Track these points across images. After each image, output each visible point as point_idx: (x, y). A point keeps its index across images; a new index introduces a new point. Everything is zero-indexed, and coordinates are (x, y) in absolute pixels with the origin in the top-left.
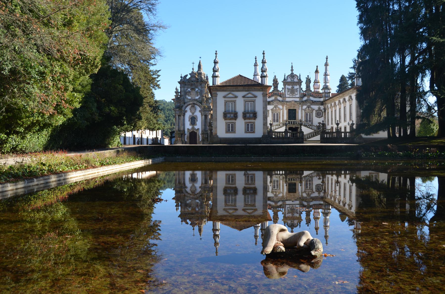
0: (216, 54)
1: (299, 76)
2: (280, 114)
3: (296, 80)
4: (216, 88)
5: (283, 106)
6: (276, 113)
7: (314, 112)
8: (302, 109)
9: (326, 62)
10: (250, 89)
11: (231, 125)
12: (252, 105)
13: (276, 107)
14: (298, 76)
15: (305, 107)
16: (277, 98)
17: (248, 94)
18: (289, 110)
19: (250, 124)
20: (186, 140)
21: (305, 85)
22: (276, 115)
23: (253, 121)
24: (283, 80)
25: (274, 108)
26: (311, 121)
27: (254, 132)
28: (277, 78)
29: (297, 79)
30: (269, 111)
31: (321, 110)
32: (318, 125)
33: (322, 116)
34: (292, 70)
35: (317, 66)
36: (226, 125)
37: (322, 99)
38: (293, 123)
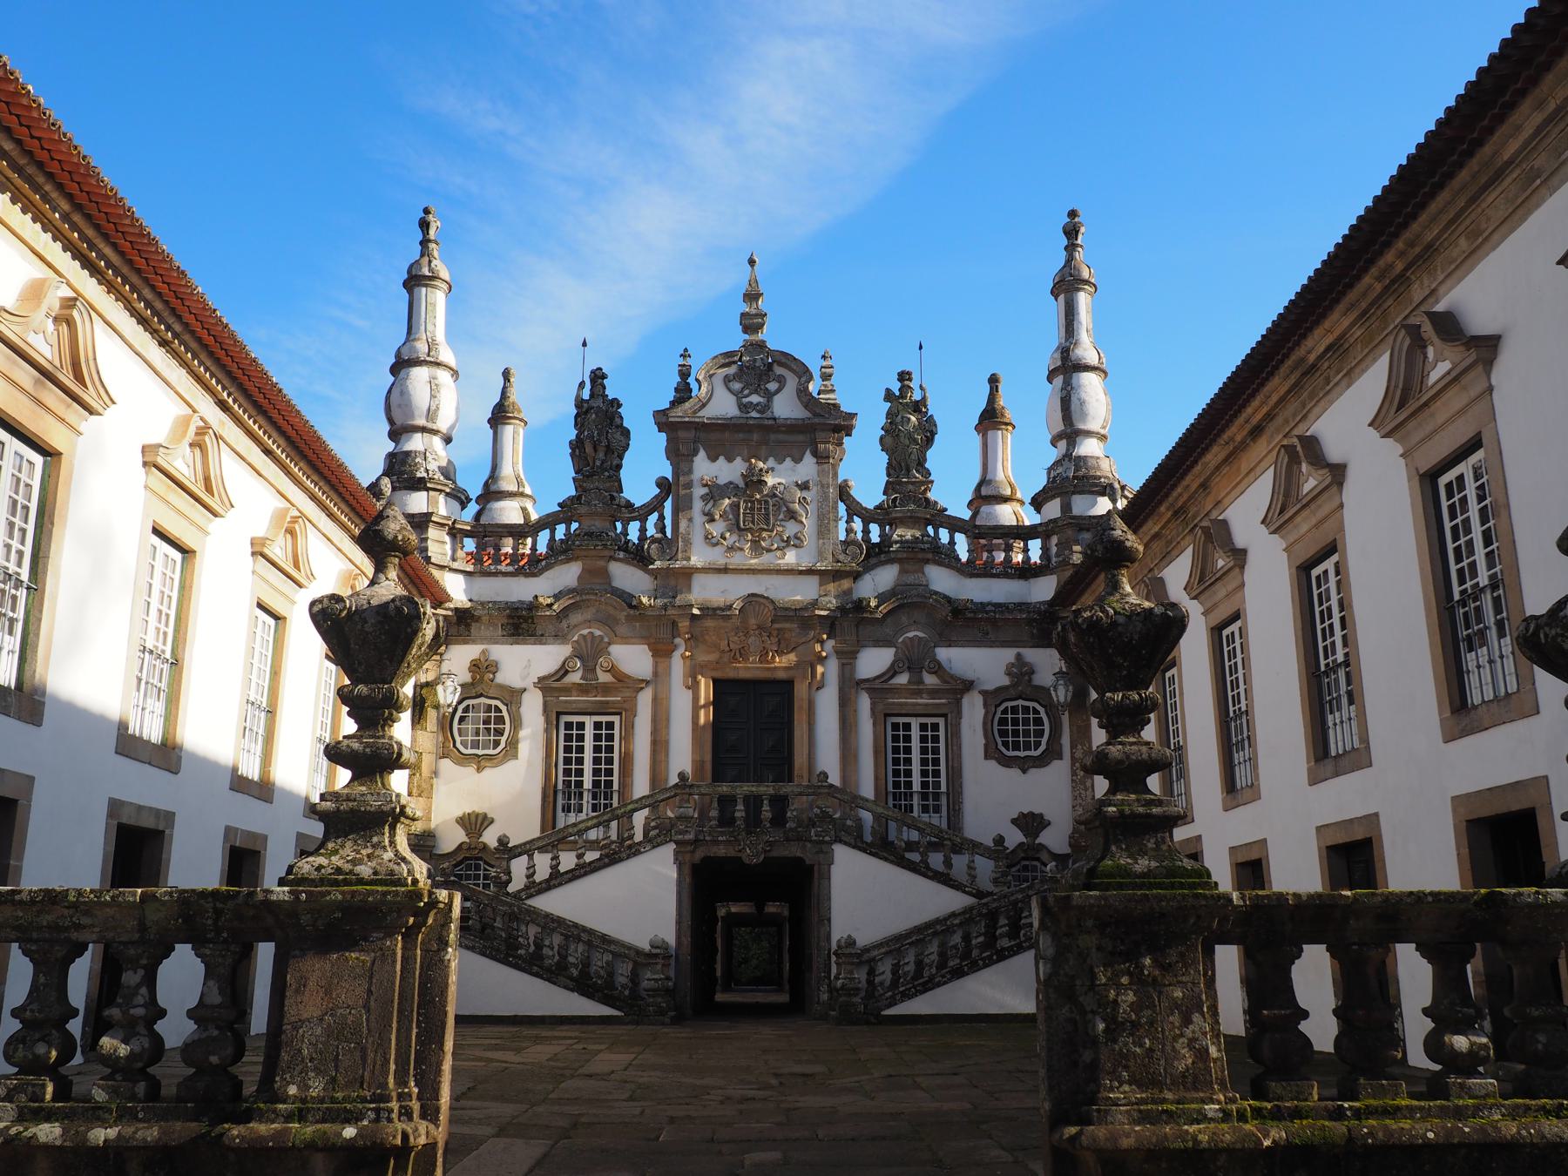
1: (814, 366)
2: (628, 729)
3: (785, 407)
5: (661, 652)
6: (589, 721)
7: (973, 712)
8: (850, 686)
9: (1070, 259)
13: (589, 655)
14: (804, 373)
15: (873, 661)
16: (605, 575)
18: (722, 687)
21: (884, 458)
22: (589, 743)
24: (664, 399)
25: (563, 671)
28: (611, 393)
29: (803, 392)
30: (513, 696)
31: (1042, 694)
32: (1014, 838)
33: (1053, 753)
34: (751, 323)
35: (994, 381)
37: (1044, 590)
38: (740, 811)
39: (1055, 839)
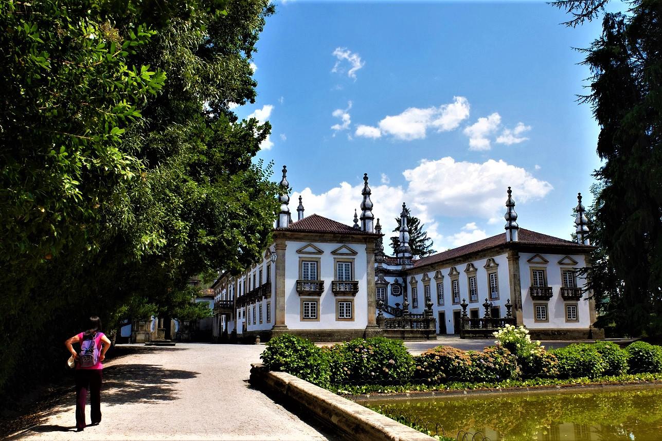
0: (284, 171)
4: (284, 234)
10: (346, 240)
11: (310, 306)
12: (349, 268)
17: (341, 248)
19: (345, 303)
20: (152, 331)
23: (351, 298)
26: (386, 300)
27: (352, 319)
31: (400, 285)
32: (395, 307)
33: (401, 294)
36: (302, 305)
37: (399, 268)
39: (401, 307)
